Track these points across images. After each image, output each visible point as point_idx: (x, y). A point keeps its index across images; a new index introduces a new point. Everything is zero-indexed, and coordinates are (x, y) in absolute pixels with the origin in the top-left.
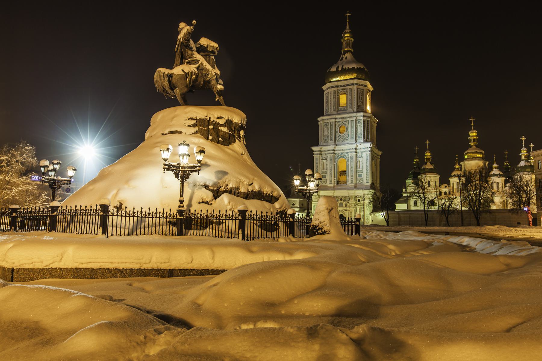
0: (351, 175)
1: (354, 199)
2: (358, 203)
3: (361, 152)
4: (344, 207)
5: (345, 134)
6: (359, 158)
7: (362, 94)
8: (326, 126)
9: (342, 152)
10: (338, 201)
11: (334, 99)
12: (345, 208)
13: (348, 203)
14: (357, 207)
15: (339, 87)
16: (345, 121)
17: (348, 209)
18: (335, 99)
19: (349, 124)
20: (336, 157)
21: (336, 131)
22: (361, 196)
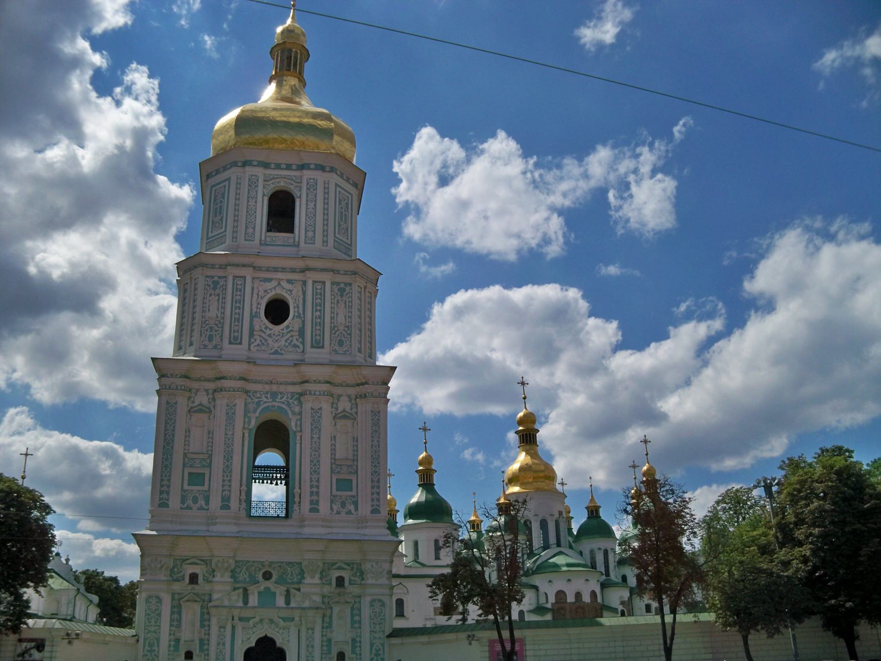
0: (311, 481)
1: (321, 573)
2: (338, 590)
5: (288, 327)
6: (341, 418)
7: (347, 204)
8: (215, 288)
9: (275, 388)
11: (252, 203)
13: (299, 590)
14: (331, 608)
17: (297, 614)
18: (256, 202)
19: (304, 293)
20: (251, 406)
21: (254, 310)
22: (348, 564)
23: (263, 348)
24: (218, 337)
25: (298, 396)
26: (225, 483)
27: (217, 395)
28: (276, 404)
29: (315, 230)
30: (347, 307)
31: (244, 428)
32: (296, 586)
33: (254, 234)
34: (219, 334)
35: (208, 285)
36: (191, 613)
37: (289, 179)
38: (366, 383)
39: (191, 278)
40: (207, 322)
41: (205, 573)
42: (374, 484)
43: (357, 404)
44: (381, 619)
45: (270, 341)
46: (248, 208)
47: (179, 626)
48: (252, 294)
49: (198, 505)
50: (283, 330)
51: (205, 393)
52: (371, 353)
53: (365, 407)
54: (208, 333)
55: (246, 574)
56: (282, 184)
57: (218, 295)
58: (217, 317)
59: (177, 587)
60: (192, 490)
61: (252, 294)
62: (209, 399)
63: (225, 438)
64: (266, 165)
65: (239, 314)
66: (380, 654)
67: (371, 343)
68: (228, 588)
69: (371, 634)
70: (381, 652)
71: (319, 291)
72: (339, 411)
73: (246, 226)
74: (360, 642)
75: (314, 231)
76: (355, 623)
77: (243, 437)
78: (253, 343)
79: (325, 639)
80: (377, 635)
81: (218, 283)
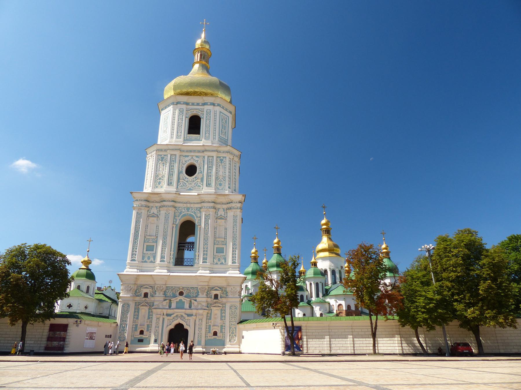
0: (204, 248)
2: (215, 301)
3: (223, 209)
4: (185, 309)
5: (196, 177)
7: (226, 121)
9: (188, 205)
10: (175, 296)
12: (189, 312)
14: (211, 310)
15: (189, 105)
16: (197, 157)
17: (194, 312)
18: (182, 121)
19: (204, 162)
21: (180, 170)
23: (184, 187)
24: (163, 182)
25: (199, 209)
26: (163, 250)
27: (161, 209)
28: (189, 213)
29: (209, 133)
30: (224, 168)
31: (173, 224)
32: (195, 299)
33: (181, 135)
34: (163, 181)
35: (159, 159)
36: (144, 311)
37: (198, 110)
38: (231, 203)
39: (152, 156)
40: (158, 176)
41: (151, 292)
42: (233, 250)
43: (227, 213)
44: (235, 315)
45: (187, 183)
46: (178, 123)
47: (137, 318)
48: (180, 162)
49: (150, 261)
50: (193, 179)
51: (156, 208)
52: (235, 189)
53: (230, 214)
54: (158, 181)
55: (171, 293)
56: (195, 112)
57: (164, 163)
58: (163, 173)
59: (137, 299)
60: (147, 253)
61: (180, 162)
62: (157, 211)
63: (164, 229)
64: (187, 104)
65: (173, 172)
66: (234, 333)
67: (235, 184)
68: (162, 299)
69: (230, 323)
70: (234, 332)
71: (210, 161)
72: (218, 216)
73: (178, 132)
74: (225, 326)
75: (209, 134)
76: (222, 318)
77: (173, 228)
78: (179, 185)
79: (208, 324)
80: (233, 323)
81: (164, 158)
